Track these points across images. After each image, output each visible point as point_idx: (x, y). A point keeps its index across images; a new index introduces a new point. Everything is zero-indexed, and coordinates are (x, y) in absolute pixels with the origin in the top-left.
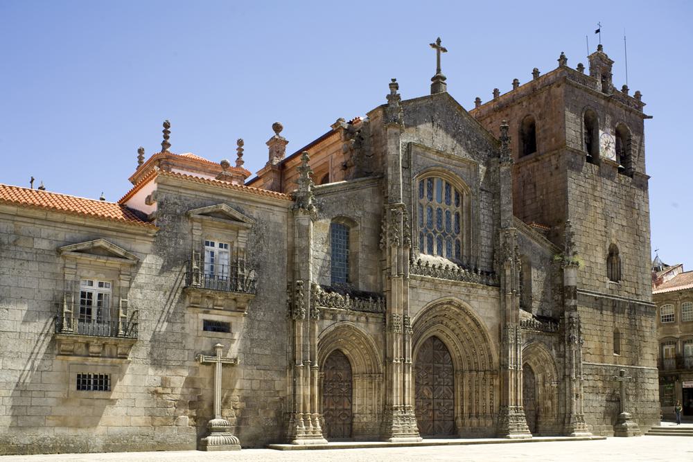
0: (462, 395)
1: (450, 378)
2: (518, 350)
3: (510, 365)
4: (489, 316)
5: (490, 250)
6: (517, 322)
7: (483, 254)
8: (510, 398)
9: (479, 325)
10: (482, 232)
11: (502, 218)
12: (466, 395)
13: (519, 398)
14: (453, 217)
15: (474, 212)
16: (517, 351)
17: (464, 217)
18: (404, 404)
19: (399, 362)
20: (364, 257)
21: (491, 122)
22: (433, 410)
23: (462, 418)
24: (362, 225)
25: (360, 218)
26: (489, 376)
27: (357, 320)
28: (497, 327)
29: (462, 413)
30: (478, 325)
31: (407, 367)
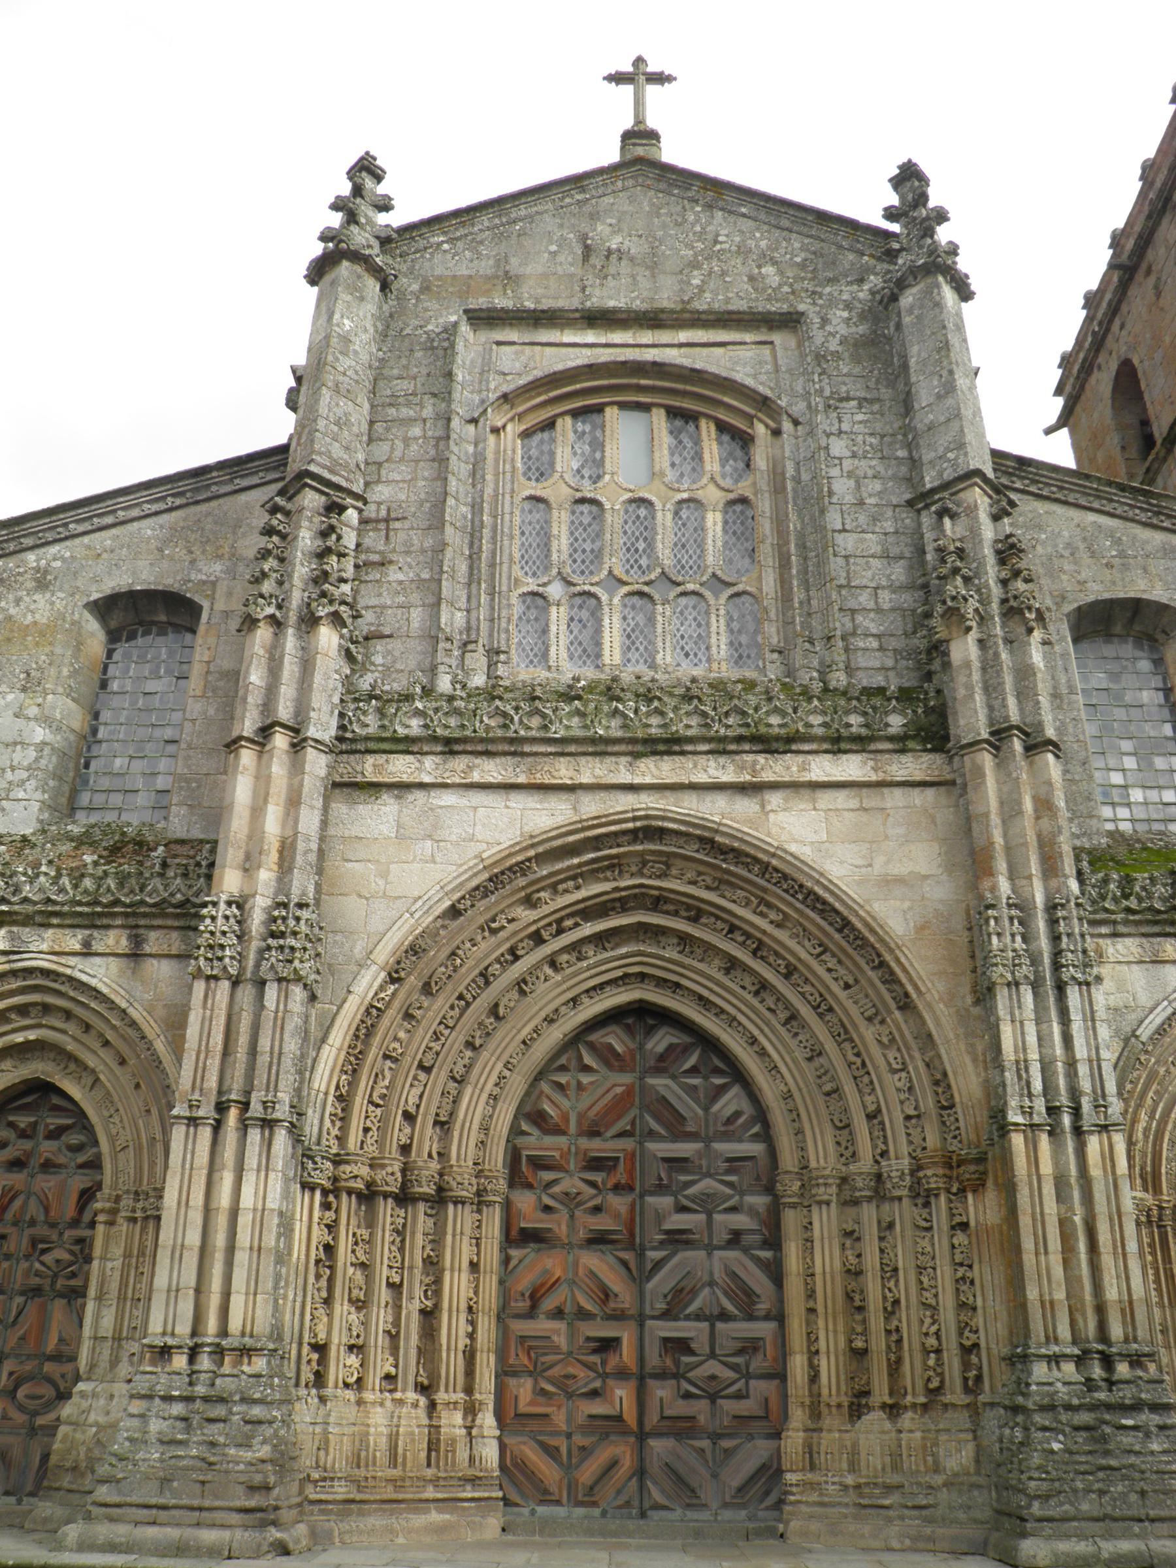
0: (811, 1295)
1: (752, 1212)
2: (1076, 1017)
3: (1013, 1103)
4: (897, 869)
5: (907, 599)
6: (1050, 867)
7: (868, 623)
8: (1032, 1294)
9: (847, 923)
10: (846, 543)
11: (927, 456)
12: (830, 1290)
13: (1112, 1293)
14: (714, 521)
15: (805, 477)
16: (1065, 1020)
17: (764, 505)
18: (224, 1332)
19: (206, 1110)
20: (211, 712)
21: (1122, 327)
22: (642, 1379)
23: (815, 1413)
24: (220, 605)
25: (214, 584)
26: (933, 1177)
27: (87, 944)
28: (959, 923)
29: (815, 1396)
30: (845, 925)
31: (255, 1135)
